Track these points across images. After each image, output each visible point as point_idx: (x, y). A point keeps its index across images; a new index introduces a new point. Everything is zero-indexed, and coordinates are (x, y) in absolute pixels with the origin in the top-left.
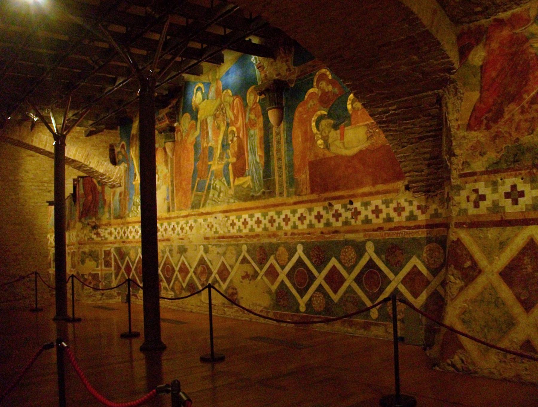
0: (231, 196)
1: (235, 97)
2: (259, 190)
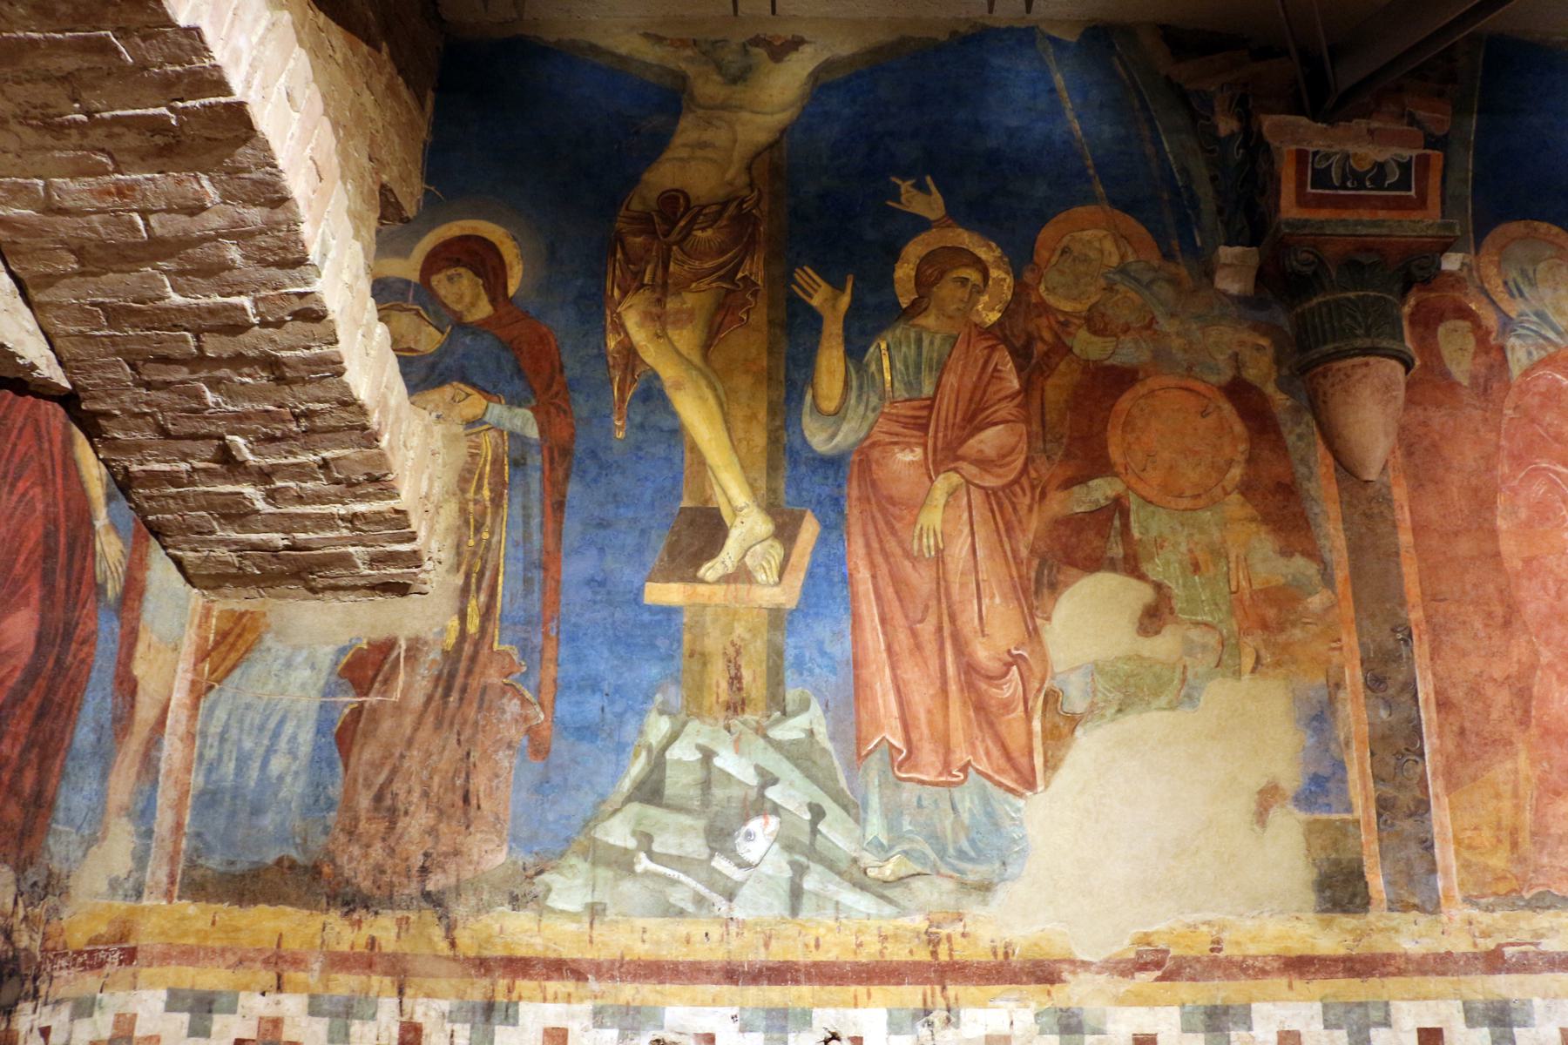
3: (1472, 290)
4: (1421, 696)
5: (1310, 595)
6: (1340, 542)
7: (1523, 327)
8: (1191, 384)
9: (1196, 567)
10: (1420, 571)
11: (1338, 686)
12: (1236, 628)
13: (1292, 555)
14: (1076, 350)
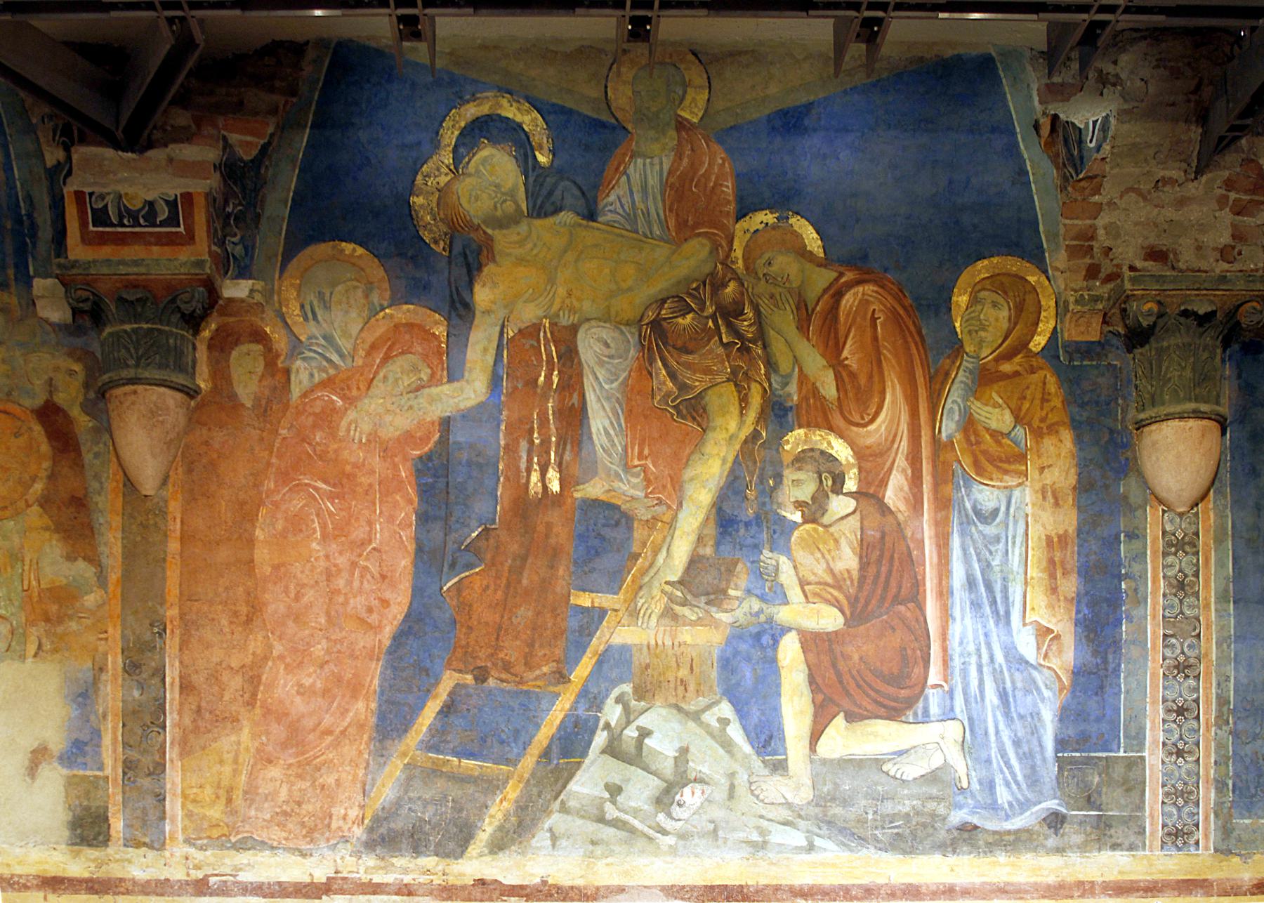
4: (168, 679)
6: (118, 549)
11: (101, 669)
13: (76, 559)
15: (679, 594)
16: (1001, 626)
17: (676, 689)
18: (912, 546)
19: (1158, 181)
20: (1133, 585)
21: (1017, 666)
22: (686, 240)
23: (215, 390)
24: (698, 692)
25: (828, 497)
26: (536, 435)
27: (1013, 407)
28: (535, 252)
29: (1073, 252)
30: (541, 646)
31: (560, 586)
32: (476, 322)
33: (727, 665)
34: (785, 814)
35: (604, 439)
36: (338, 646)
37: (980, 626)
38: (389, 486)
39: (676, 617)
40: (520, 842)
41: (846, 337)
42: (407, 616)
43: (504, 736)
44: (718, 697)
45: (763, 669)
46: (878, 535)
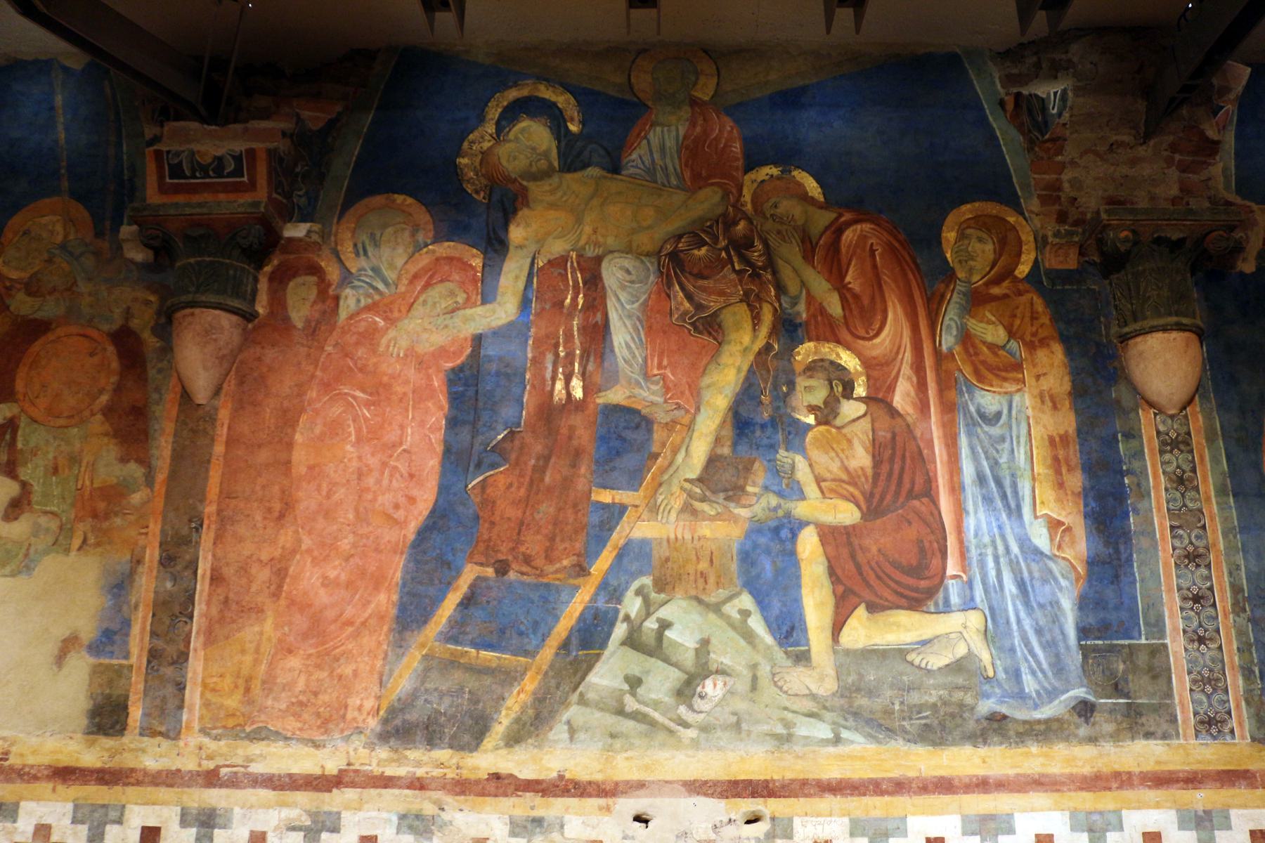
0: (810, 705)
1: (847, 216)
2: (1052, 694)
3: (326, 251)
5: (134, 492)
7: (359, 280)
8: (90, 331)
9: (56, 470)
10: (223, 474)
11: (139, 562)
12: (73, 516)
13: (128, 461)
14: (12, 308)
15: (698, 490)
16: (1013, 519)
17: (696, 581)
18: (922, 445)
19: (1112, 145)
20: (1135, 480)
21: (1032, 556)
22: (700, 188)
23: (272, 314)
24: (718, 584)
25: (839, 401)
26: (561, 349)
27: (1006, 324)
28: (564, 199)
29: (1044, 200)
30: (562, 541)
31: (581, 484)
32: (509, 255)
33: (747, 558)
34: (810, 705)
35: (626, 353)
36: (364, 541)
37: (993, 519)
38: (422, 394)
39: (694, 512)
40: (537, 735)
41: (849, 264)
42: (433, 512)
43: (523, 628)
44: (738, 589)
45: (783, 561)
46: (889, 436)
